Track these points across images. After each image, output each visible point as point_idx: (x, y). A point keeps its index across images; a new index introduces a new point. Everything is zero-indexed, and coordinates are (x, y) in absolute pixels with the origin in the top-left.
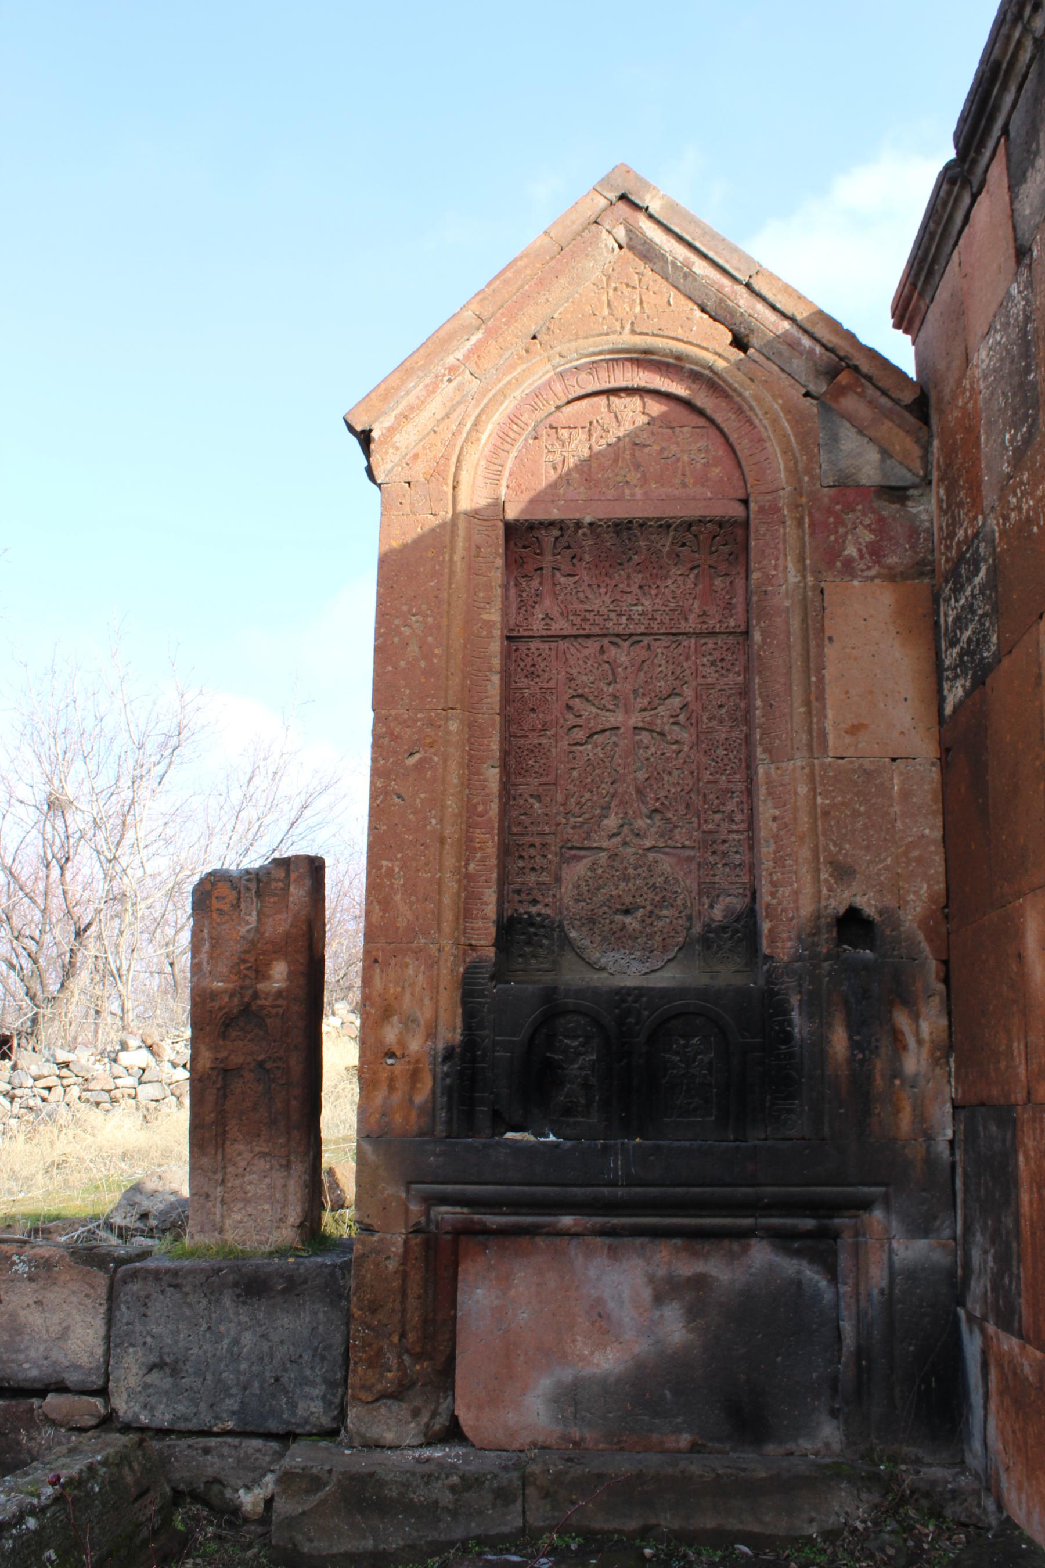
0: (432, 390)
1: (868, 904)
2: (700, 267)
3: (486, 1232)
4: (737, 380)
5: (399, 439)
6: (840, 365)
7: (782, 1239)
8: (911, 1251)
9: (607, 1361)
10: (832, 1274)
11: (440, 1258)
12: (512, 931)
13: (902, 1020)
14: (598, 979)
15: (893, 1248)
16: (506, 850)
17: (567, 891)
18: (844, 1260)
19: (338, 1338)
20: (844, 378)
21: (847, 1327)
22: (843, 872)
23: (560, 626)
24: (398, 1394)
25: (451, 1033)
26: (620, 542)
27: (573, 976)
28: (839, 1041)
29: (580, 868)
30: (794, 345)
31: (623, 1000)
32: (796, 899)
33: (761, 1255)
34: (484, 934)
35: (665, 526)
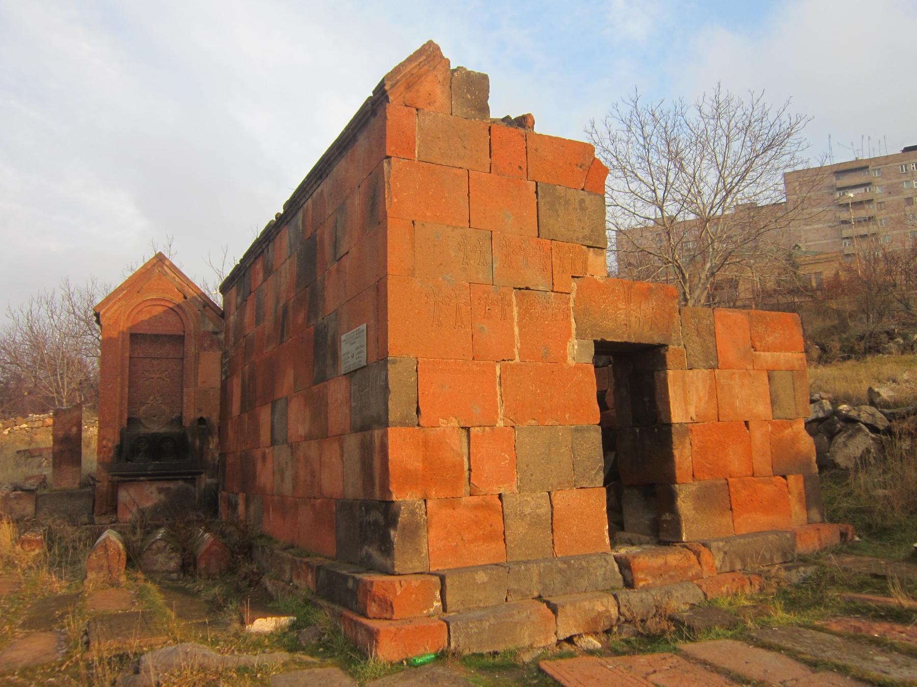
0: (115, 303)
1: (204, 416)
2: (177, 279)
3: (125, 481)
4: (184, 305)
5: (108, 315)
6: (207, 303)
7: (185, 480)
8: (209, 481)
9: (149, 504)
10: (194, 486)
11: (115, 487)
12: (130, 420)
13: (210, 439)
14: (147, 430)
15: (206, 480)
16: (129, 404)
17: (141, 412)
18: (197, 483)
19: (91, 504)
20: (207, 308)
21: (197, 496)
22: (200, 410)
23: (141, 355)
24: (105, 514)
25: (117, 442)
26: (156, 338)
27: (142, 430)
28: (198, 442)
29: (144, 407)
30: (197, 299)
31: (155, 435)
32: (190, 415)
33: (181, 483)
34: (125, 422)
35: (166, 336)
